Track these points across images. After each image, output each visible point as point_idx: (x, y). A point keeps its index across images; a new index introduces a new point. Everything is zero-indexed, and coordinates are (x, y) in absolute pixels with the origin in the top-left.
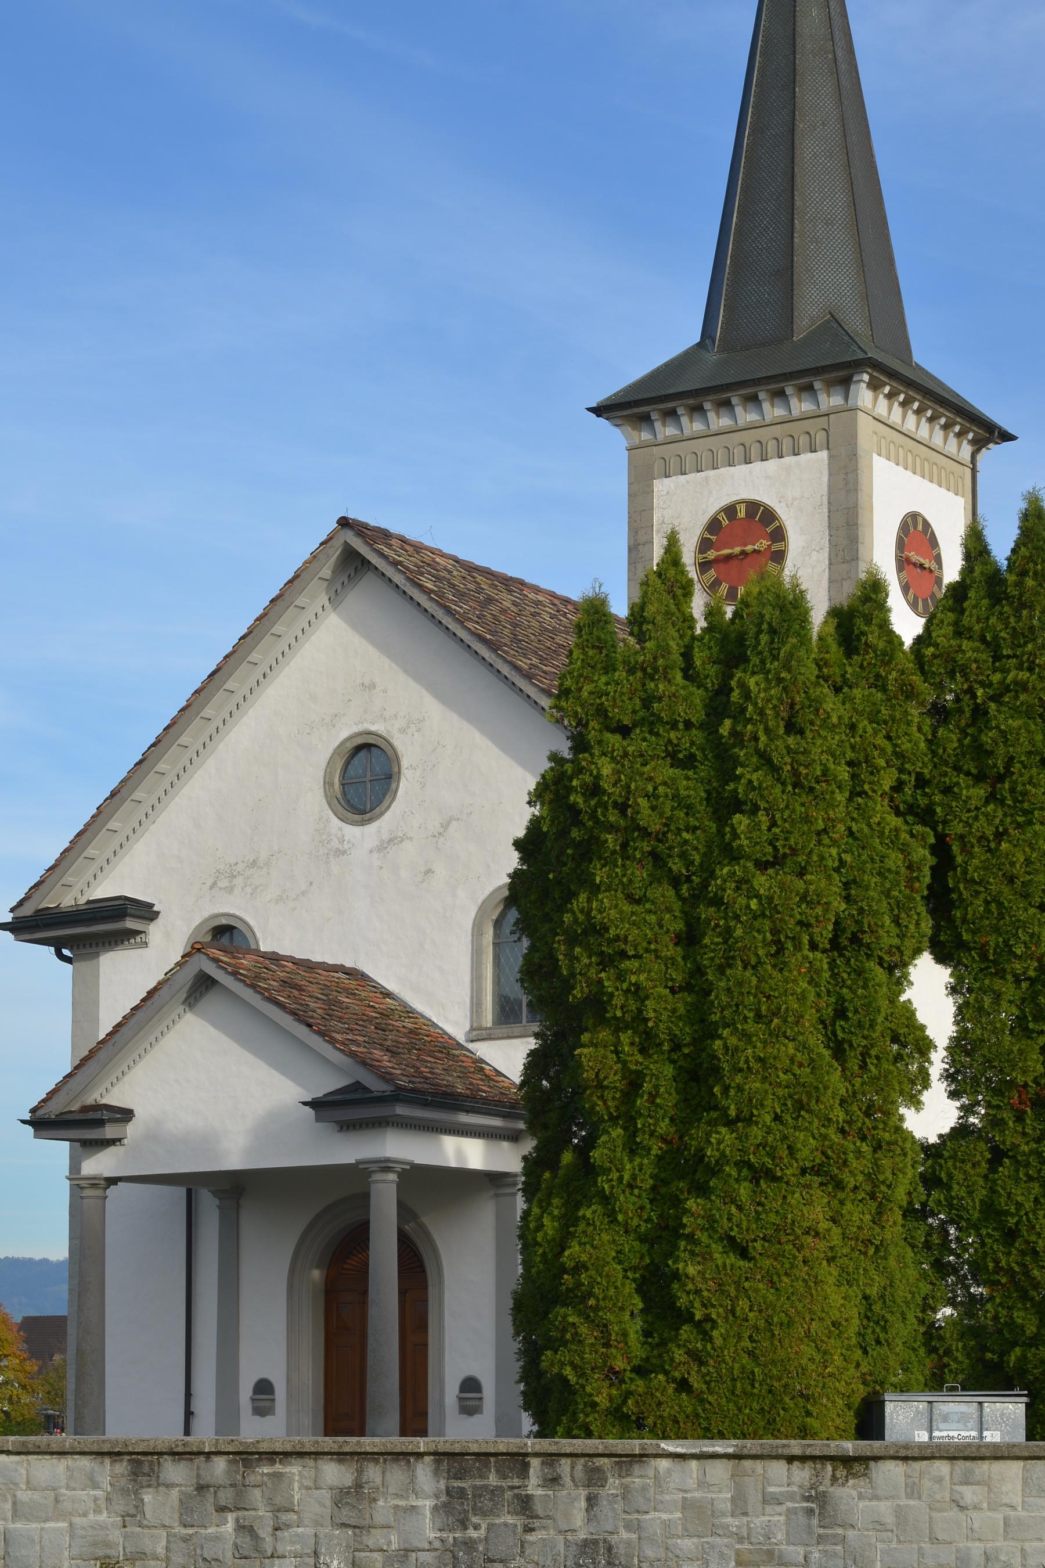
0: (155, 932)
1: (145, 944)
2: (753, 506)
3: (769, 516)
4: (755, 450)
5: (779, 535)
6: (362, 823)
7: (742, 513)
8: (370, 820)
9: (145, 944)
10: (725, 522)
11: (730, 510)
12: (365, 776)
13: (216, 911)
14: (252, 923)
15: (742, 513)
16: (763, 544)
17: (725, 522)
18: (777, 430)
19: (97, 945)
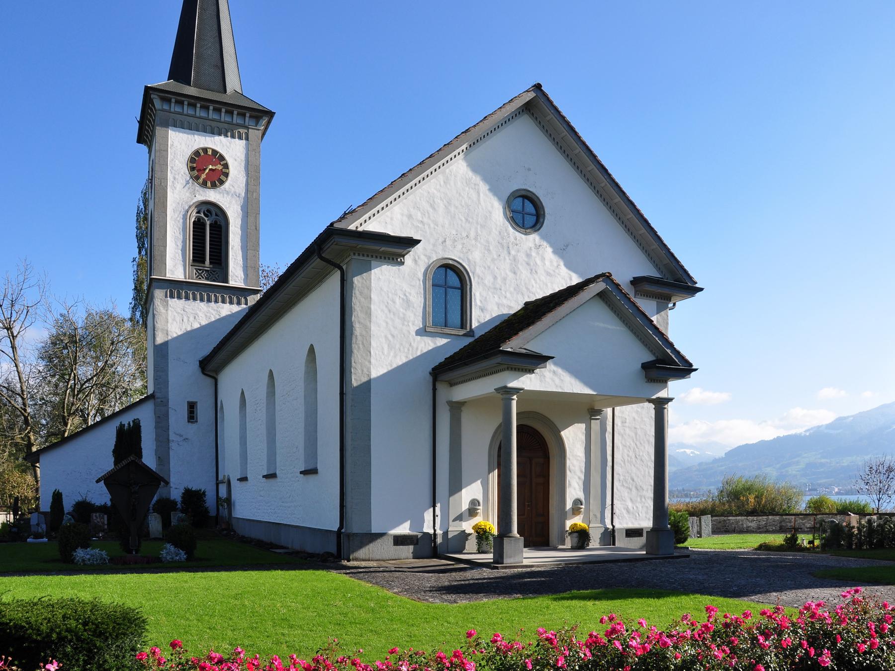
1: (403, 263)
2: (215, 152)
3: (222, 158)
4: (216, 130)
5: (226, 166)
7: (210, 153)
9: (403, 263)
10: (202, 154)
11: (205, 150)
13: (446, 256)
14: (467, 267)
15: (210, 153)
16: (219, 167)
17: (202, 154)
18: (226, 126)
19: (372, 256)
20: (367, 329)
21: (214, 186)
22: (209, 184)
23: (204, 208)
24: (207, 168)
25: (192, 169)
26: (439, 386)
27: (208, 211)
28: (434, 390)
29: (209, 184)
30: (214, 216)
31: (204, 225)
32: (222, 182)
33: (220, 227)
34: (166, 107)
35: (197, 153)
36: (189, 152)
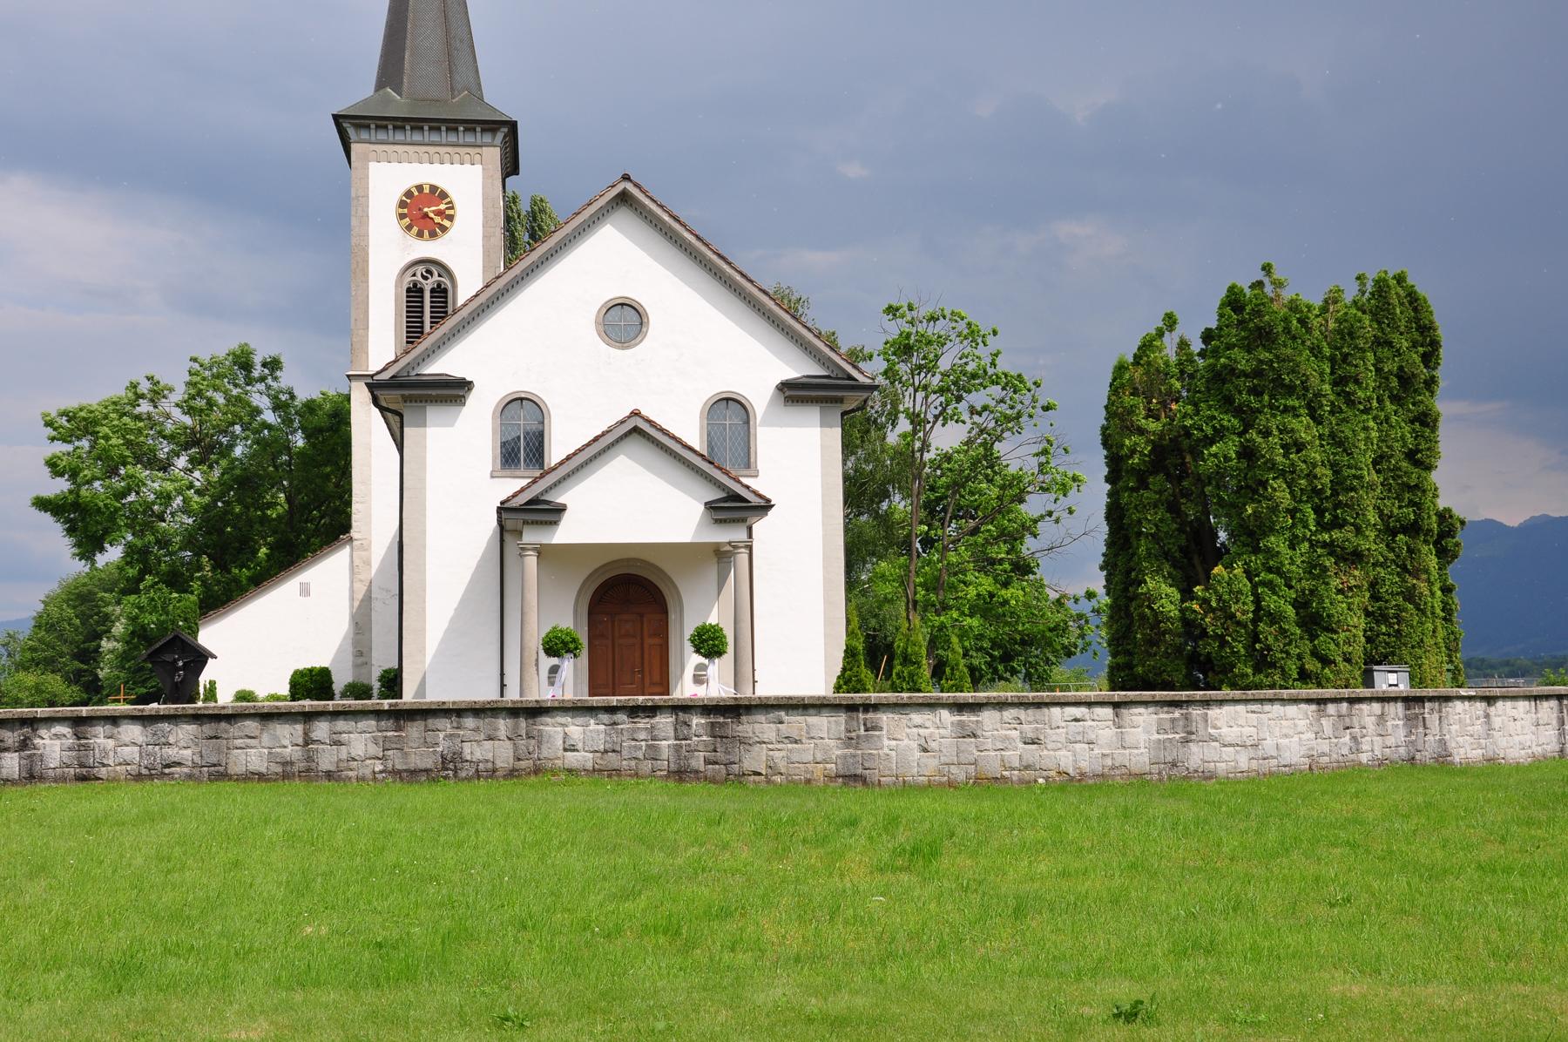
0: (472, 399)
2: (433, 188)
6: (623, 348)
7: (427, 190)
8: (628, 348)
11: (420, 188)
12: (624, 321)
15: (427, 190)
20: (423, 480)
21: (433, 235)
22: (426, 233)
23: (421, 269)
24: (424, 211)
25: (402, 216)
26: (507, 537)
27: (429, 271)
28: (502, 541)
29: (426, 233)
30: (436, 277)
31: (421, 291)
32: (444, 229)
33: (445, 291)
34: (364, 135)
35: (409, 194)
36: (397, 194)
